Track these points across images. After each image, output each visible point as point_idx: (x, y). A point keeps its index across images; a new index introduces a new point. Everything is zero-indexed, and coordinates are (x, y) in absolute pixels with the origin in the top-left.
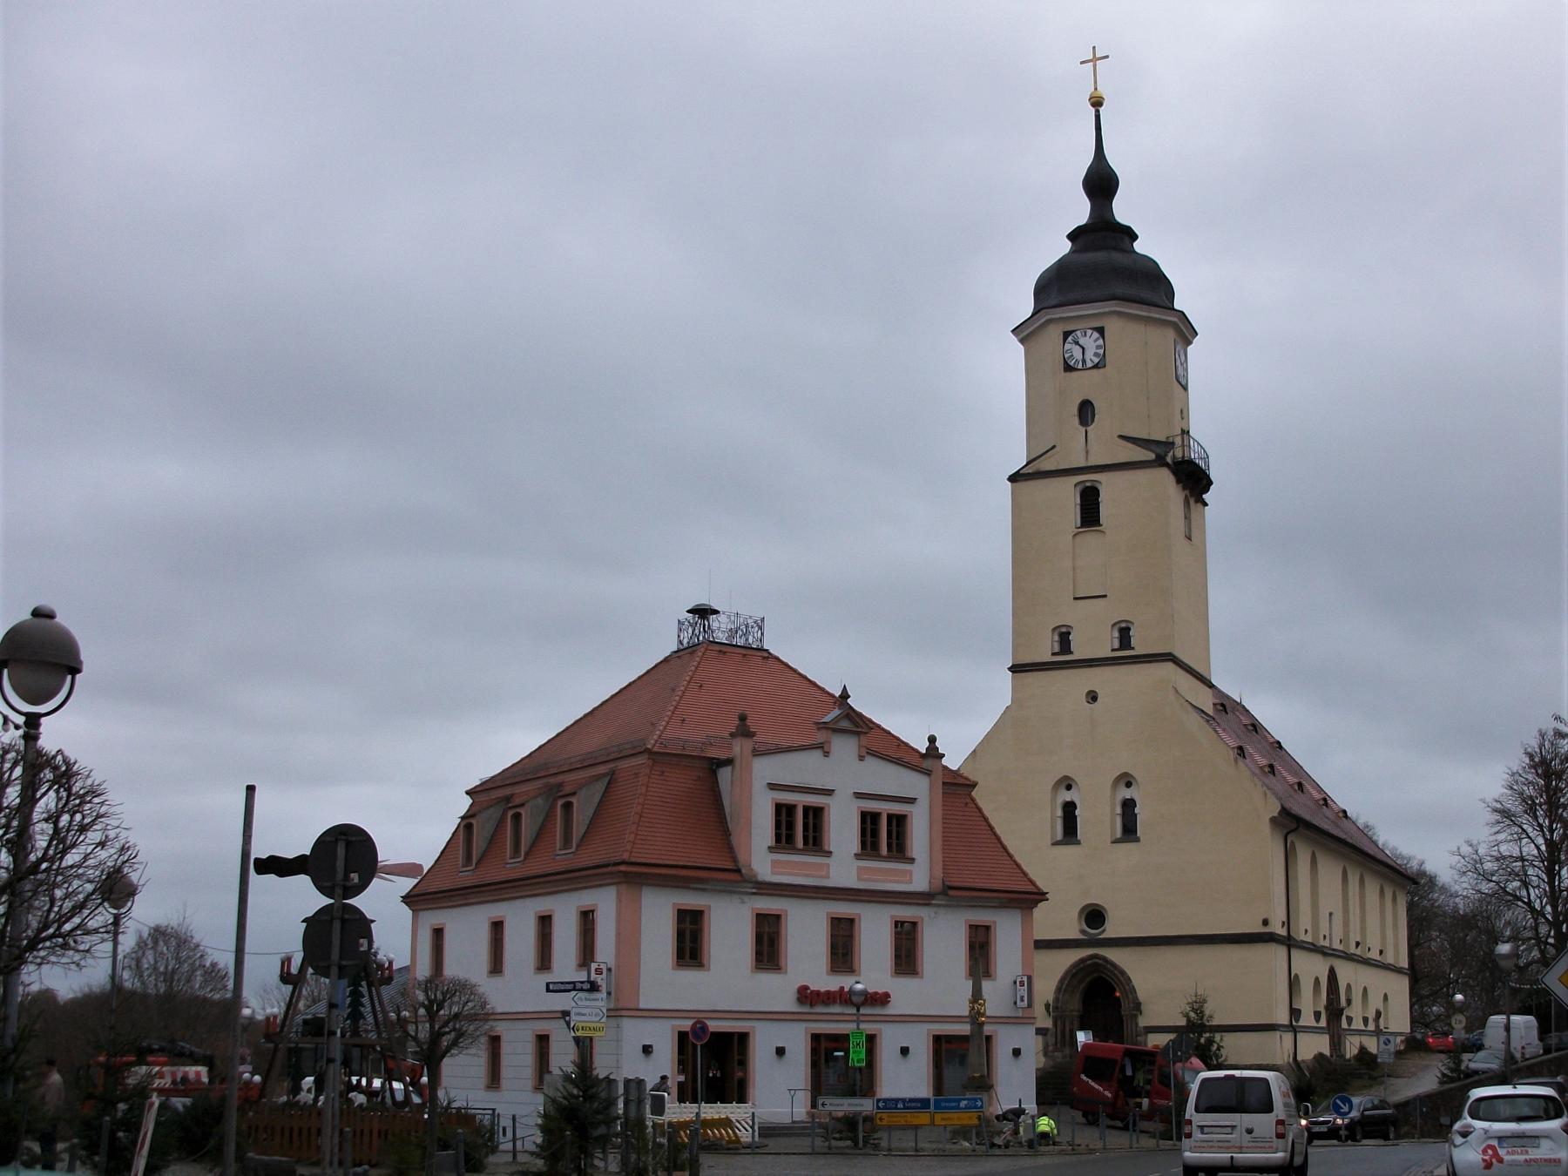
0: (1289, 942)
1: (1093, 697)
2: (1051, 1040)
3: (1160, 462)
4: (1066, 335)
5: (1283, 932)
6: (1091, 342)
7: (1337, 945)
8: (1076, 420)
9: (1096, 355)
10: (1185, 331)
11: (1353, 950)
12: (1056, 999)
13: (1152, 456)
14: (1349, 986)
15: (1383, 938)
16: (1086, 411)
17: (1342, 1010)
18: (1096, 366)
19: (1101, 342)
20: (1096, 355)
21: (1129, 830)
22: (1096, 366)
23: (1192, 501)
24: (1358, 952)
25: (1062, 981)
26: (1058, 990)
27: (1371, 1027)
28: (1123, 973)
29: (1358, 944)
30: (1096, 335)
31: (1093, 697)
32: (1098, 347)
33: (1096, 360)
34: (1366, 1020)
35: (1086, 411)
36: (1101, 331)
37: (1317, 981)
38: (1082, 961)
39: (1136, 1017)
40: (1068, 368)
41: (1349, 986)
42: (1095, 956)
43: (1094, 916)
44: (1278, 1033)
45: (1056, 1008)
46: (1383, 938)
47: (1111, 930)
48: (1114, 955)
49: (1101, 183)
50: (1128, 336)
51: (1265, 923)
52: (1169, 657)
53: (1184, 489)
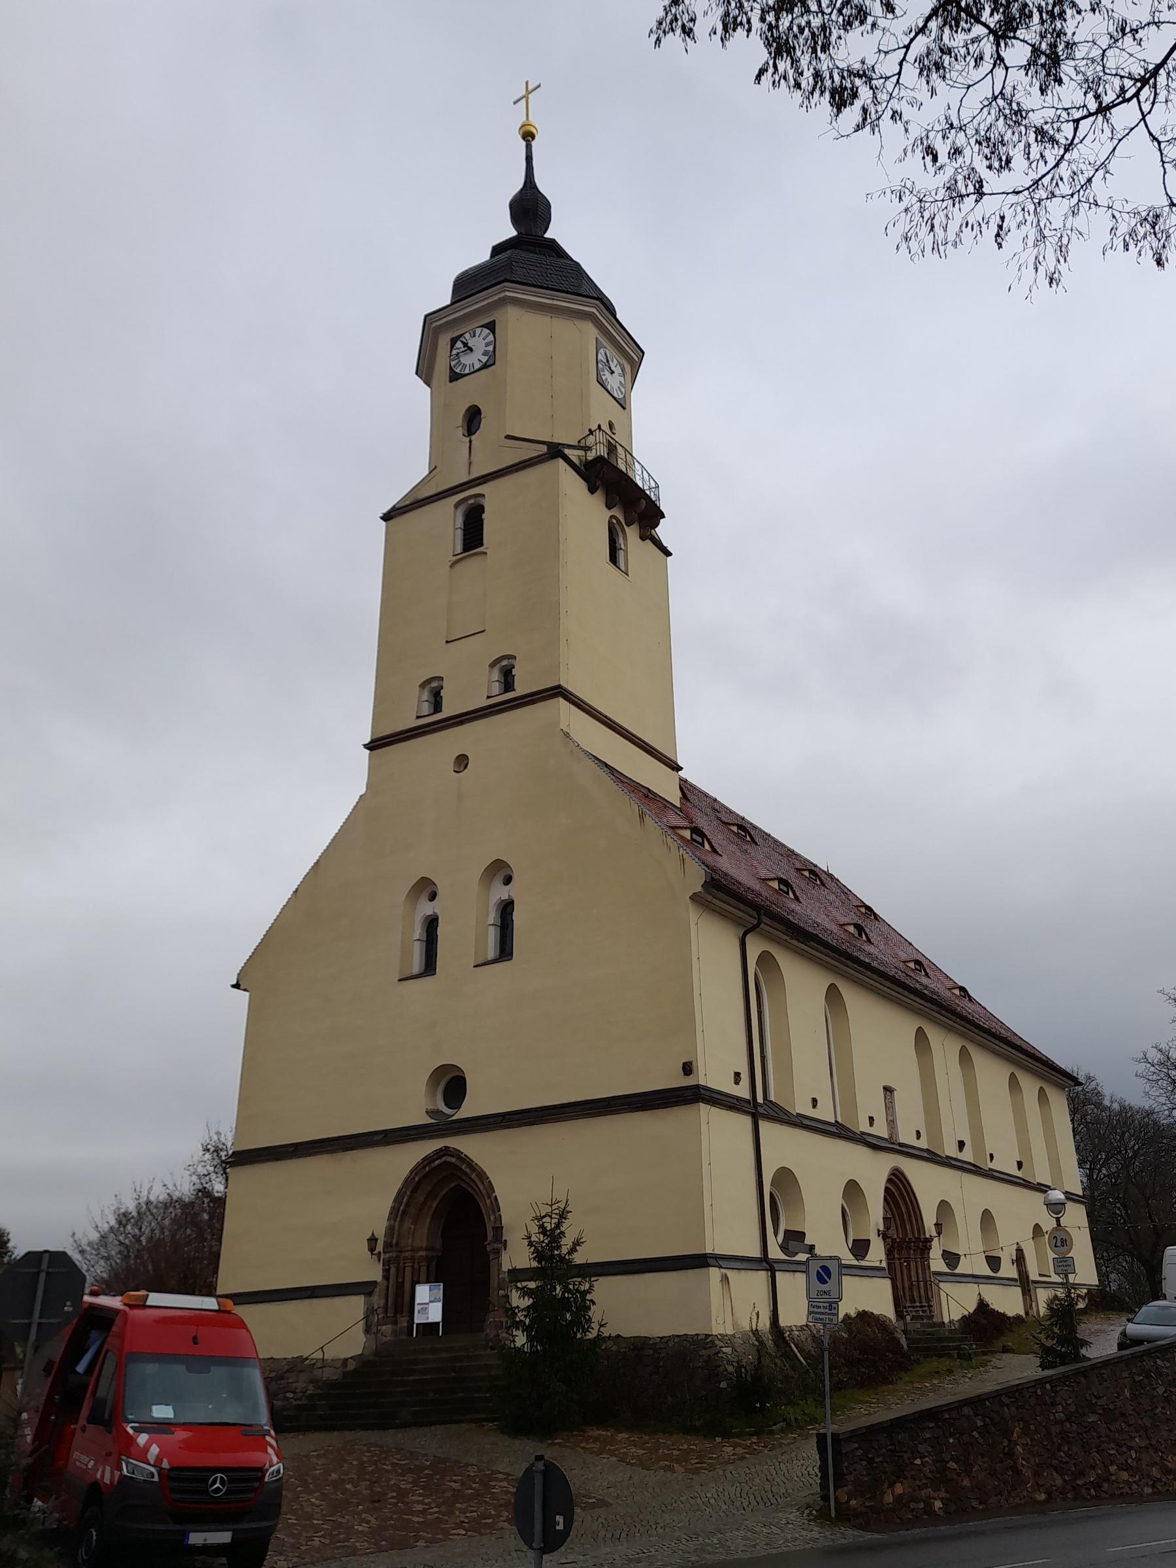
0: (759, 1110)
1: (462, 761)
2: (377, 1301)
3: (555, 451)
4: (453, 342)
5: (743, 1091)
6: (480, 342)
7: (906, 1136)
8: (460, 431)
9: (485, 353)
10: (632, 356)
11: (951, 1150)
12: (390, 1230)
13: (544, 448)
14: (944, 1207)
15: (1024, 1143)
16: (473, 418)
17: (930, 1240)
18: (485, 366)
19: (491, 338)
20: (485, 353)
21: (505, 951)
22: (485, 366)
23: (632, 533)
24: (967, 1155)
25: (398, 1199)
26: (394, 1213)
27: (1008, 1270)
28: (482, 1175)
29: (961, 1144)
30: (486, 331)
31: (462, 761)
32: (487, 345)
33: (484, 359)
34: (994, 1262)
35: (473, 418)
36: (491, 326)
37: (852, 1190)
38: (427, 1160)
39: (498, 1253)
40: (454, 377)
41: (944, 1207)
42: (445, 1151)
43: (453, 1085)
44: (714, 1273)
45: (388, 1245)
46: (1024, 1143)
47: (470, 1108)
48: (470, 1146)
49: (530, 208)
50: (529, 332)
51: (688, 1069)
52: (560, 691)
53: (609, 506)
